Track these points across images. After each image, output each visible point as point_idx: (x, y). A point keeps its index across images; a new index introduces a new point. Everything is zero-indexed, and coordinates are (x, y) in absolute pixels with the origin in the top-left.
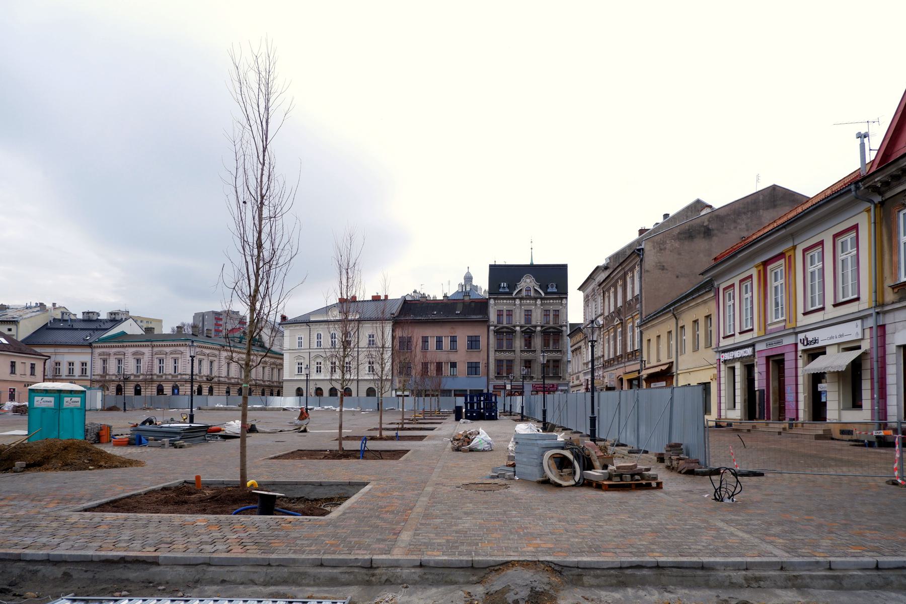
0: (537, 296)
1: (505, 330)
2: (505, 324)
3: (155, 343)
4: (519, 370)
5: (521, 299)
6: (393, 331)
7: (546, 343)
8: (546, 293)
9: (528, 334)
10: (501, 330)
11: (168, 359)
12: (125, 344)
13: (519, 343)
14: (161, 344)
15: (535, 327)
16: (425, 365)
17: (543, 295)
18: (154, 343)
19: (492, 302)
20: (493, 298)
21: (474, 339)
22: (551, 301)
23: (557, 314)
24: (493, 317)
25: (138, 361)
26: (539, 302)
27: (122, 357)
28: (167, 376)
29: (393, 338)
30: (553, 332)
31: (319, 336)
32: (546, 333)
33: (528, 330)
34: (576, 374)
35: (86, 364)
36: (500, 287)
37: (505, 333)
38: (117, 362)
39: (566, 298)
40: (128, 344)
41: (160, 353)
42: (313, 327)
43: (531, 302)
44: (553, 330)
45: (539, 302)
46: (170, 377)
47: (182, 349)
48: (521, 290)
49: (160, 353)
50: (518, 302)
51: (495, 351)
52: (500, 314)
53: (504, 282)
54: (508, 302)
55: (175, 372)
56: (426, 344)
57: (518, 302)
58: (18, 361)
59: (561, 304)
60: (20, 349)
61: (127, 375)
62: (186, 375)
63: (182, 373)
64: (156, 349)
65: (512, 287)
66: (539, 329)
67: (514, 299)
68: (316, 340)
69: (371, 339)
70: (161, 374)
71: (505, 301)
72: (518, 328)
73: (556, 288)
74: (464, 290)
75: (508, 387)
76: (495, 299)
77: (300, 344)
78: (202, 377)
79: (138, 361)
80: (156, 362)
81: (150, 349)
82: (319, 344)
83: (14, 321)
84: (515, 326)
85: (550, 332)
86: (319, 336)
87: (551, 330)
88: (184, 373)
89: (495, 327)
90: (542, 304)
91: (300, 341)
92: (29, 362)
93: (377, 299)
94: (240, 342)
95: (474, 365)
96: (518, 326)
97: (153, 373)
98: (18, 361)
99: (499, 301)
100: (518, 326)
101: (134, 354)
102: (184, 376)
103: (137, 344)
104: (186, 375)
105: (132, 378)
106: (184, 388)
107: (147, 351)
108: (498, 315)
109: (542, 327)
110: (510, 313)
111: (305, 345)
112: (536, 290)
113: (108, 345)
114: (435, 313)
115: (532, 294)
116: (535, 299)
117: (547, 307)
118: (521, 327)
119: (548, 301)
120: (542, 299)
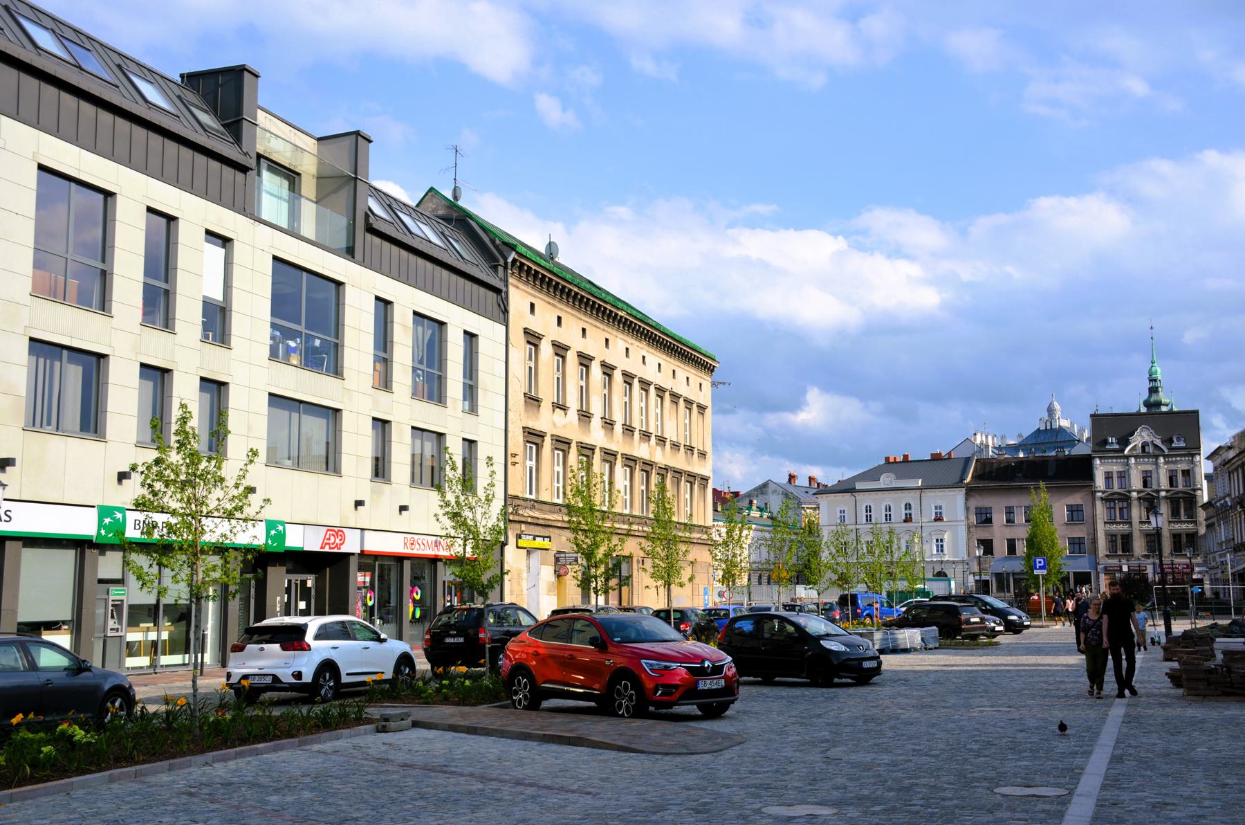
0: (1157, 452)
1: (1116, 496)
2: (1116, 489)
4: (1139, 546)
5: (1136, 457)
6: (966, 499)
7: (1175, 513)
8: (1171, 449)
9: (1151, 503)
10: (1111, 497)
13: (1136, 512)
15: (1158, 491)
16: (1012, 545)
17: (1166, 451)
19: (1097, 461)
20: (1099, 457)
21: (1075, 508)
22: (1179, 459)
23: (1186, 473)
24: (1100, 482)
26: (1162, 460)
29: (967, 509)
30: (1183, 498)
31: (869, 509)
32: (1174, 501)
33: (1147, 496)
34: (1212, 553)
36: (1105, 442)
37: (1118, 500)
39: (1199, 454)
42: (859, 496)
43: (1151, 460)
44: (1184, 495)
45: (1162, 460)
48: (1135, 445)
50: (1133, 460)
51: (1105, 523)
52: (1108, 476)
53: (1112, 437)
54: (1119, 461)
56: (1012, 515)
57: (1133, 460)
59: (1192, 462)
65: (1124, 442)
66: (1163, 494)
67: (1127, 457)
68: (864, 514)
69: (938, 511)
71: (1114, 460)
72: (1134, 494)
73: (1185, 441)
74: (1049, 428)
75: (1125, 568)
76: (1100, 458)
77: (843, 519)
82: (869, 519)
84: (1129, 492)
85: (1180, 498)
86: (869, 509)
87: (1180, 495)
89: (1103, 492)
90: (1166, 463)
91: (842, 514)
93: (937, 457)
95: (1077, 541)
96: (1135, 491)
99: (1106, 461)
100: (1135, 491)
108: (1106, 478)
109: (1167, 491)
110: (1123, 476)
111: (849, 519)
112: (1156, 446)
114: (1020, 475)
115: (1150, 449)
116: (1157, 457)
117: (1172, 467)
118: (1139, 492)
119: (1174, 459)
120: (1165, 456)
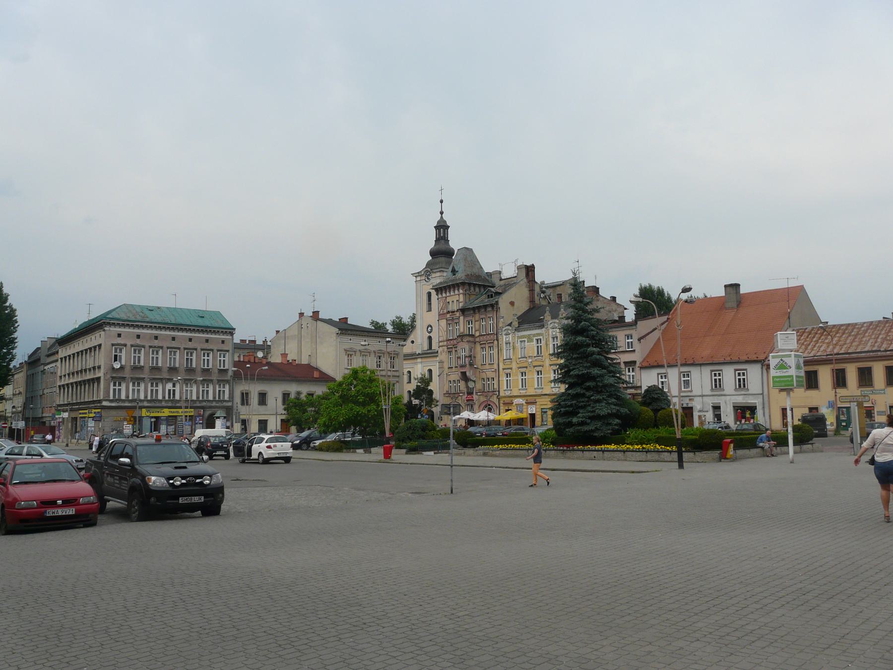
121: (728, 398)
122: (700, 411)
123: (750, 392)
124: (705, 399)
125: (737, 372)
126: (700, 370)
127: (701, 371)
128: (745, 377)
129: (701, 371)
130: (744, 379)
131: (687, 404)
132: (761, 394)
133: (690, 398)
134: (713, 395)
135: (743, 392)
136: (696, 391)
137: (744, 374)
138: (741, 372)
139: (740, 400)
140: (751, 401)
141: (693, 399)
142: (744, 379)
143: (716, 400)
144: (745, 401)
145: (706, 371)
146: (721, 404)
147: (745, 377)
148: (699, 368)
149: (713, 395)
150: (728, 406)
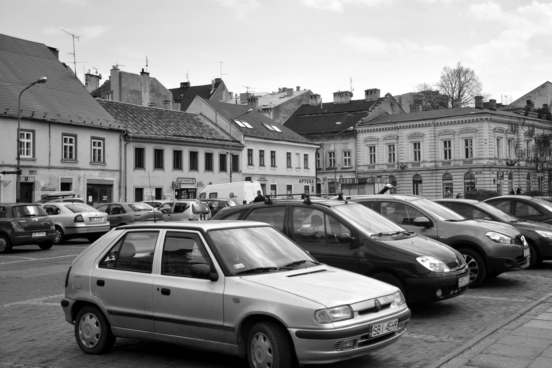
3: (439, 121)
11: (456, 140)
12: (398, 125)
14: (460, 120)
18: (437, 121)
25: (417, 145)
27: (394, 141)
28: (457, 163)
35: (349, 153)
38: (387, 147)
40: (402, 125)
41: (446, 133)
46: (461, 163)
47: (475, 126)
49: (467, 131)
55: (467, 156)
58: (293, 152)
60: (293, 138)
61: (402, 163)
62: (483, 159)
63: (478, 157)
64: (439, 129)
70: (418, 161)
78: (500, 161)
79: (417, 145)
80: (441, 146)
81: (432, 128)
83: (267, 109)
88: (481, 156)
92: (302, 152)
94: (526, 115)
97: (437, 159)
98: (293, 152)
101: (411, 137)
102: (481, 161)
103: (411, 124)
104: (483, 159)
105: (410, 167)
106: (483, 176)
107: (426, 131)
113: (375, 128)
121: (82, 173)
122: (44, 189)
123: (107, 167)
124: (53, 172)
125: (64, 137)
126: (48, 131)
127: (50, 132)
128: (93, 148)
129: (50, 132)
130: (99, 151)
131: (27, 178)
132: (117, 171)
133: (32, 169)
134: (65, 168)
135: (99, 167)
136: (42, 160)
137: (99, 144)
138: (69, 137)
139: (96, 176)
140: (108, 178)
141: (36, 171)
142: (71, 148)
143: (67, 175)
144: (102, 178)
145: (57, 134)
146: (73, 180)
147: (93, 148)
148: (47, 127)
149: (65, 168)
150: (82, 183)
